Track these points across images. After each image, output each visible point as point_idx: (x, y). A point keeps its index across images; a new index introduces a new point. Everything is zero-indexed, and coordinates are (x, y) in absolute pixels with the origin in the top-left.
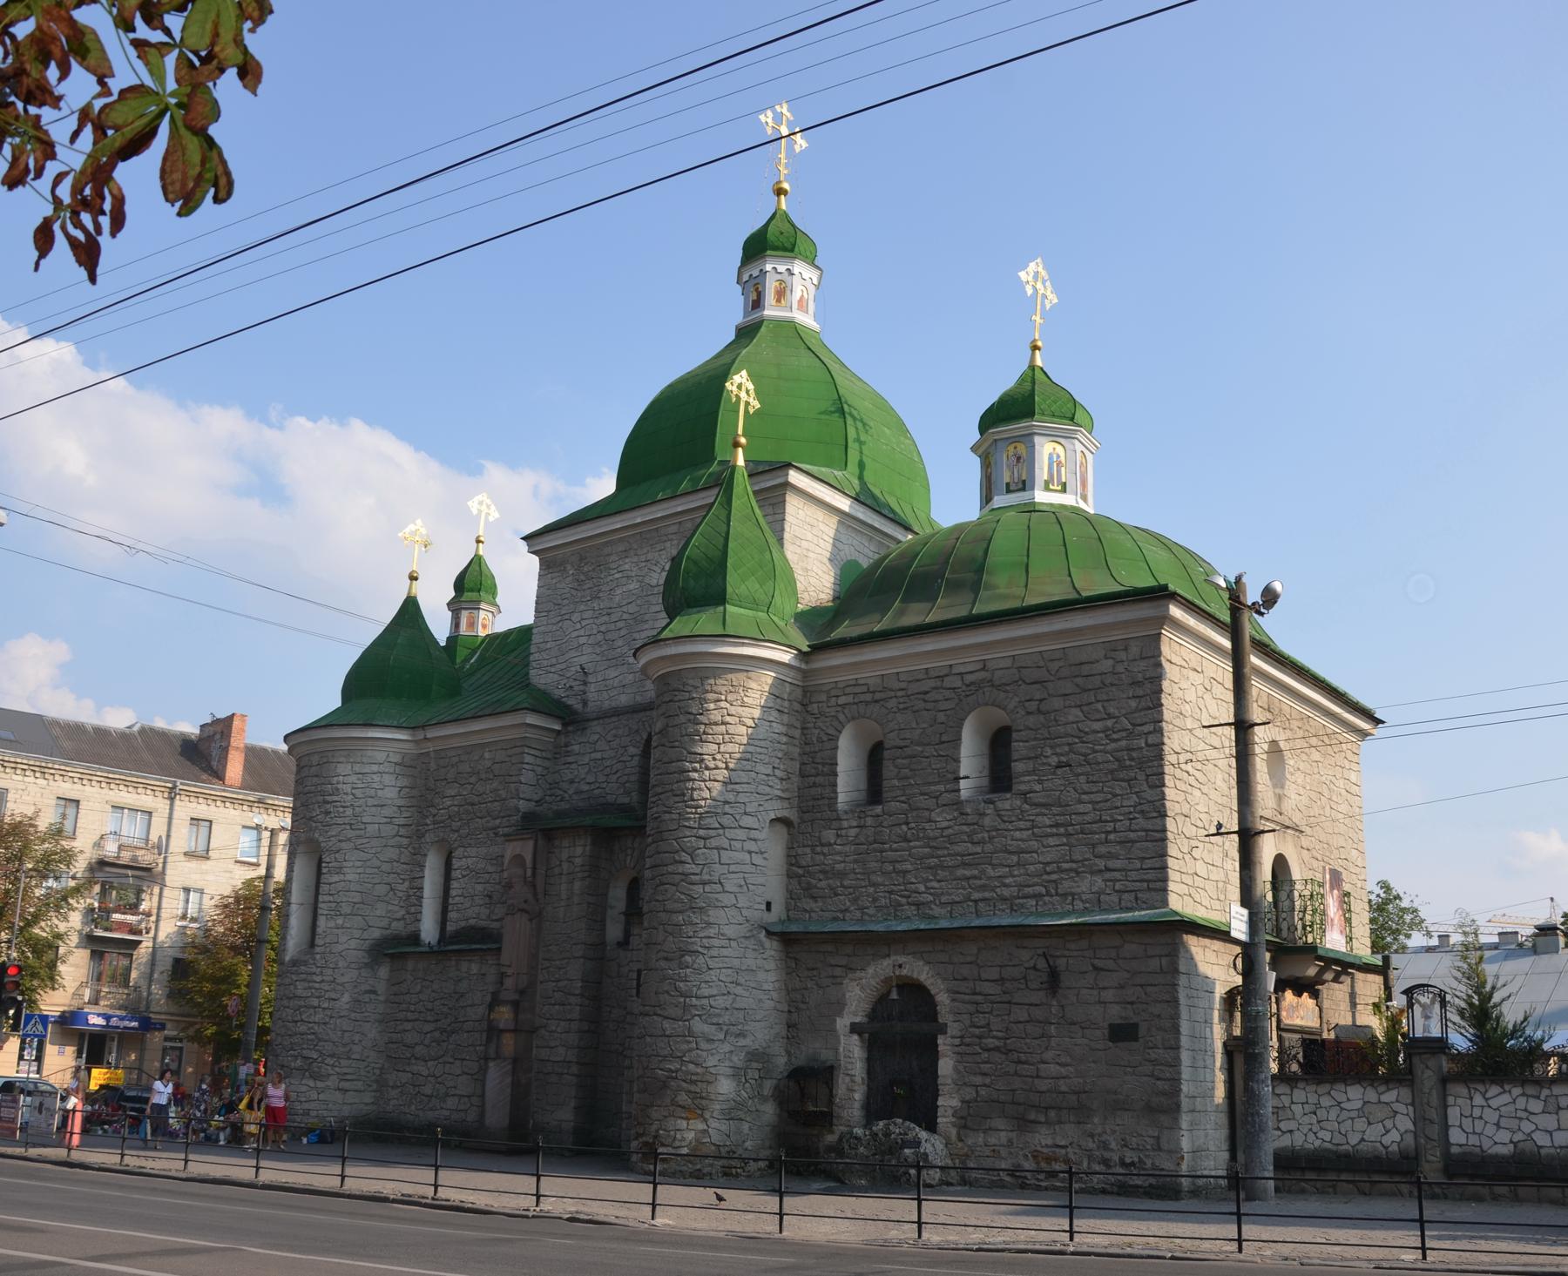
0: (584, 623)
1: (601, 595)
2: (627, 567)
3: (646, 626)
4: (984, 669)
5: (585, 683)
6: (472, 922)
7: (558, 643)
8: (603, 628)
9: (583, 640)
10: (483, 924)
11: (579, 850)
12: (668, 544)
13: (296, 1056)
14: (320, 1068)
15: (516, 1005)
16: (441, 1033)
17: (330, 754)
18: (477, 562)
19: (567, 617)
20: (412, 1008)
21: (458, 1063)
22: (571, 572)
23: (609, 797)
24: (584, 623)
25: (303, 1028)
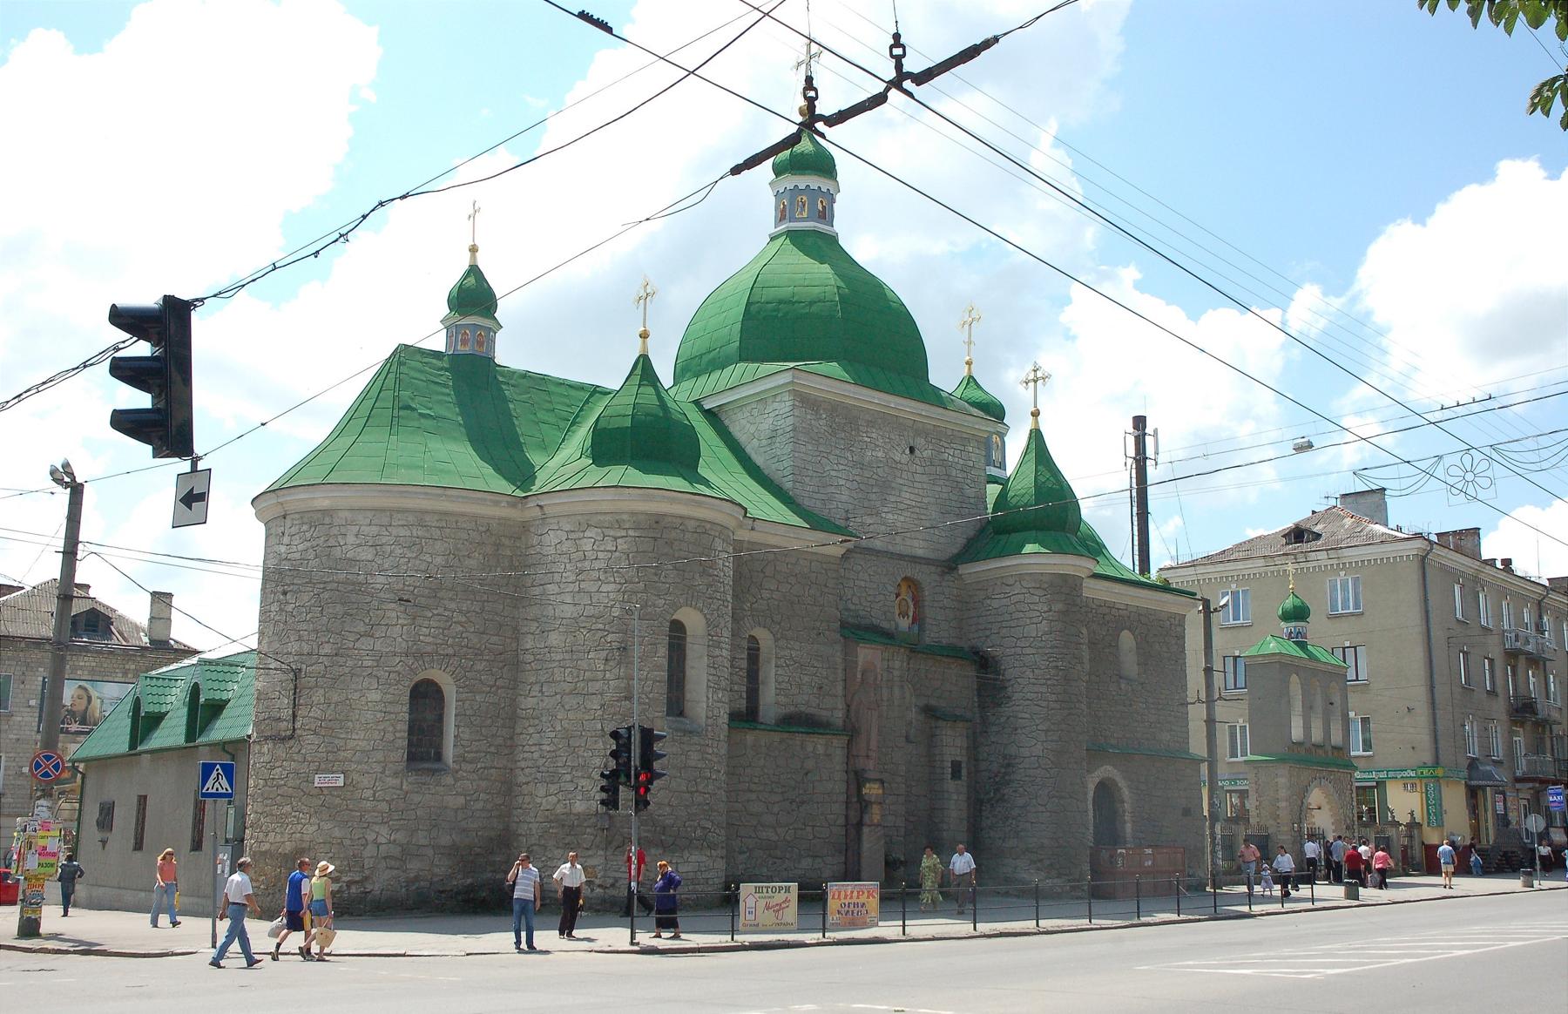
0: (841, 467)
1: (854, 450)
2: (874, 435)
3: (893, 493)
4: (1126, 610)
5: (847, 519)
6: (803, 708)
7: (820, 475)
8: (857, 478)
9: (842, 482)
10: (811, 710)
11: (897, 664)
12: (906, 433)
13: (696, 828)
14: (713, 837)
15: (882, 782)
16: (791, 803)
17: (708, 526)
18: (474, 271)
19: (825, 455)
20: (756, 780)
21: (809, 829)
22: (824, 416)
23: (873, 619)
24: (841, 467)
25: (699, 798)
